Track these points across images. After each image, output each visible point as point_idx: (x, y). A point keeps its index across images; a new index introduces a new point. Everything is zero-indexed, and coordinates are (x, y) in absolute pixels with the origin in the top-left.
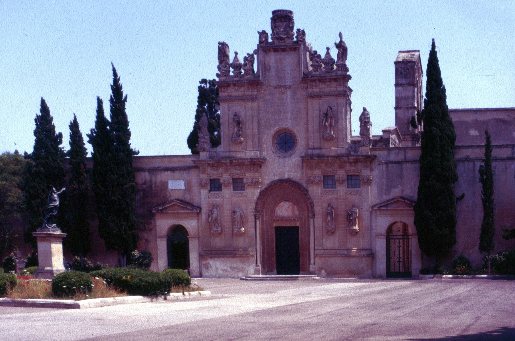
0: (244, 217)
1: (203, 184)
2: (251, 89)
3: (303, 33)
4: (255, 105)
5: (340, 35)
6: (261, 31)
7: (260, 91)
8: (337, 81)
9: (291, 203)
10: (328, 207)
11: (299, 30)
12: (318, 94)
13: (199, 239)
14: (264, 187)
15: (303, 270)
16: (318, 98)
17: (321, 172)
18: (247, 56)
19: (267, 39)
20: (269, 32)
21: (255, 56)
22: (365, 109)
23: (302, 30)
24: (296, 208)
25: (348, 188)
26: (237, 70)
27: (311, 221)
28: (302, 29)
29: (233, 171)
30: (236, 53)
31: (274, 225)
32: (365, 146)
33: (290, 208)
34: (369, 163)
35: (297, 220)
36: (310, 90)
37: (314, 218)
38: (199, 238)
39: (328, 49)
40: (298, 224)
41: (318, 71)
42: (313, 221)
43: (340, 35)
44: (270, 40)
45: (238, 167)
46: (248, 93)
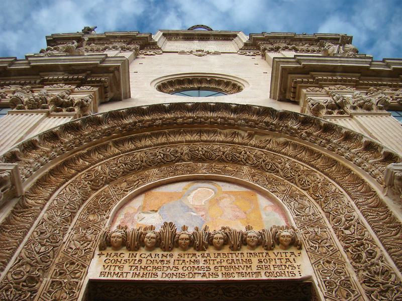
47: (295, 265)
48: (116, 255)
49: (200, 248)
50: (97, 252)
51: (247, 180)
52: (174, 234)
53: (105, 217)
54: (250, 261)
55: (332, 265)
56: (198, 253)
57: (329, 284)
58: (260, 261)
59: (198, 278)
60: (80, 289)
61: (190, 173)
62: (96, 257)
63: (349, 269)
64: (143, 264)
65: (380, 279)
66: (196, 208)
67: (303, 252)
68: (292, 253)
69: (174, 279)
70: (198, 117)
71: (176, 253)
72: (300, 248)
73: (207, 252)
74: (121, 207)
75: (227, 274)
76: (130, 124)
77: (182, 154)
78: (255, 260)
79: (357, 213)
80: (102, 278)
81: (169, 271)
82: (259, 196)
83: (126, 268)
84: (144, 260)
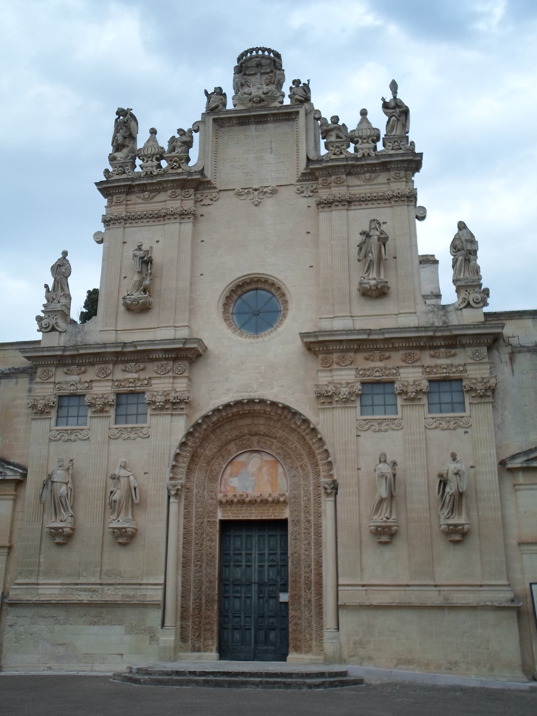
0: (137, 490)
1: (40, 406)
2: (181, 194)
3: (306, 88)
4: (187, 227)
5: (394, 86)
6: (210, 91)
7: (201, 201)
8: (388, 170)
9: (267, 458)
10: (380, 462)
11: (296, 82)
12: (344, 198)
13: (9, 554)
14: (197, 417)
15: (297, 649)
16: (344, 205)
17: (353, 372)
18: (177, 136)
19: (225, 105)
20: (229, 91)
21: (196, 136)
22: (462, 226)
23: (304, 84)
24: (280, 469)
25: (430, 412)
26: (152, 160)
27: (328, 504)
28: (304, 81)
29: (119, 375)
30: (153, 132)
31: (220, 515)
32: (472, 307)
33: (265, 470)
34: (484, 350)
35: (285, 502)
36: (324, 194)
37: (336, 494)
38: (10, 548)
39: (364, 113)
40: (286, 514)
41: (341, 153)
42: (332, 503)
43: (394, 86)
44: (230, 106)
45: (133, 364)
46: (174, 205)
47: (284, 512)
48: (225, 507)
49: (253, 504)
50: (218, 506)
51: (274, 454)
52: (243, 500)
53: (217, 484)
54: (269, 510)
55: (296, 512)
56: (252, 506)
57: (293, 521)
58: (273, 510)
59: (253, 518)
60: (217, 524)
61: (250, 448)
62: (219, 508)
63: (302, 514)
64: (235, 512)
65: (306, 523)
66: (252, 474)
67: (288, 506)
68: (284, 506)
69: (245, 518)
70: (250, 410)
71: (245, 506)
72: (287, 504)
73: (255, 505)
74: (223, 474)
75: (261, 516)
76: (216, 420)
77: (244, 433)
78: (271, 509)
79: (311, 489)
80: (223, 519)
81: (243, 515)
82: (279, 465)
83: (230, 514)
84: (235, 509)
